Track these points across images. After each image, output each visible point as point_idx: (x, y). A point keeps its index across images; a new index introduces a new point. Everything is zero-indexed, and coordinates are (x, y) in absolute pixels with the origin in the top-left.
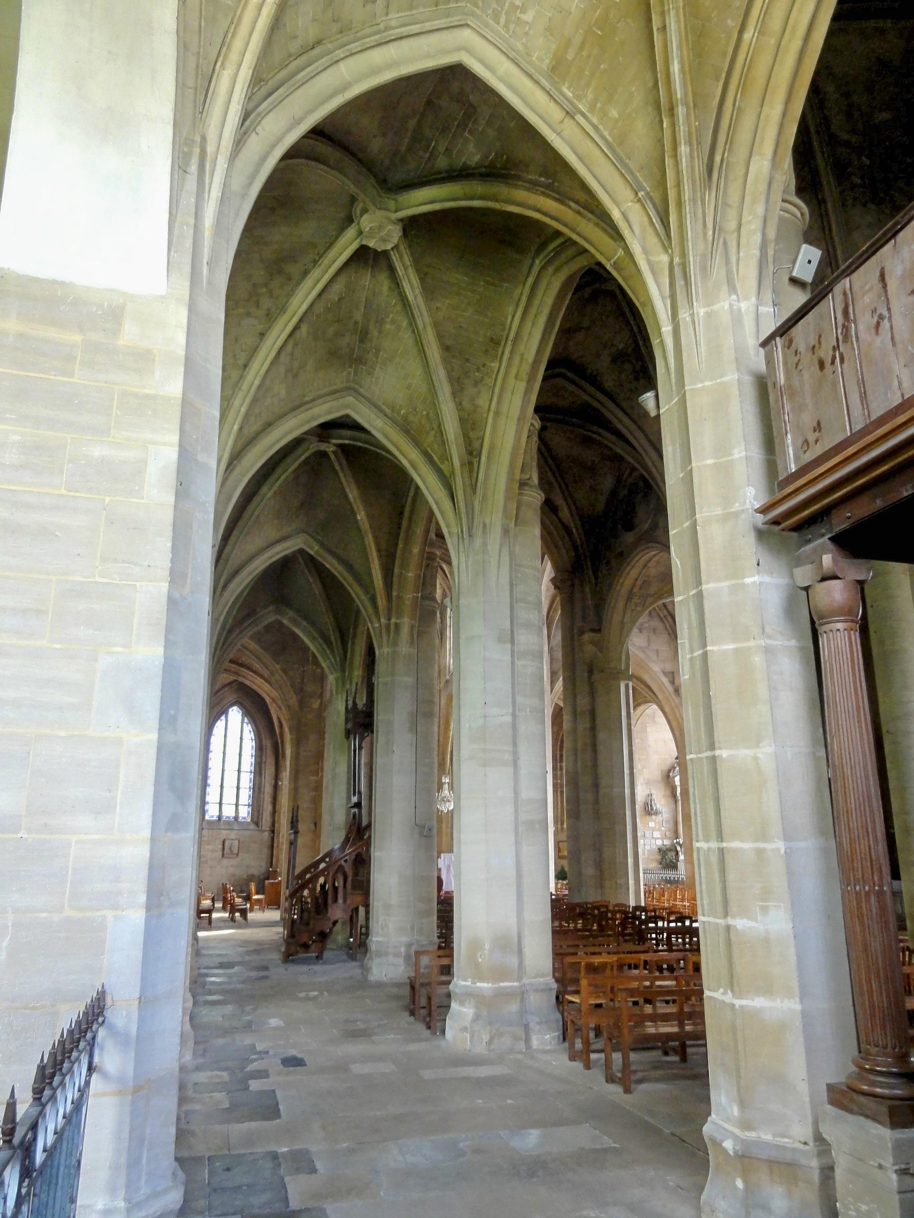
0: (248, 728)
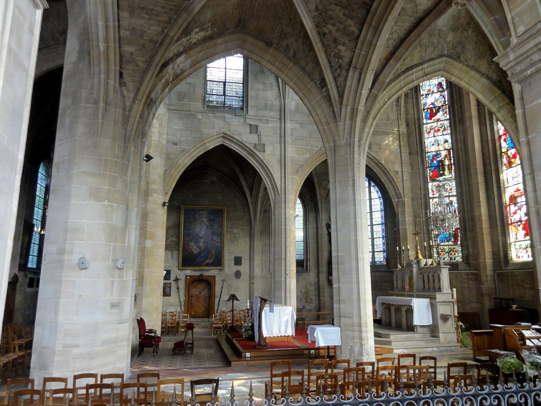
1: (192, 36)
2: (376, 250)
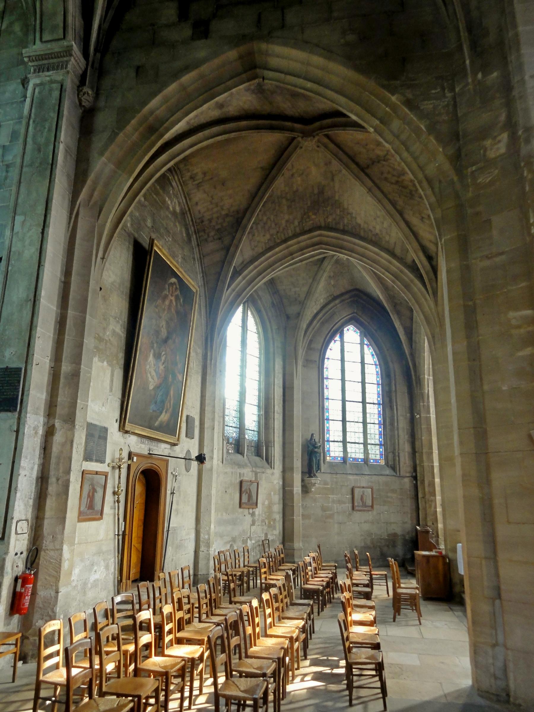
0: (368, 352)
2: (369, 441)
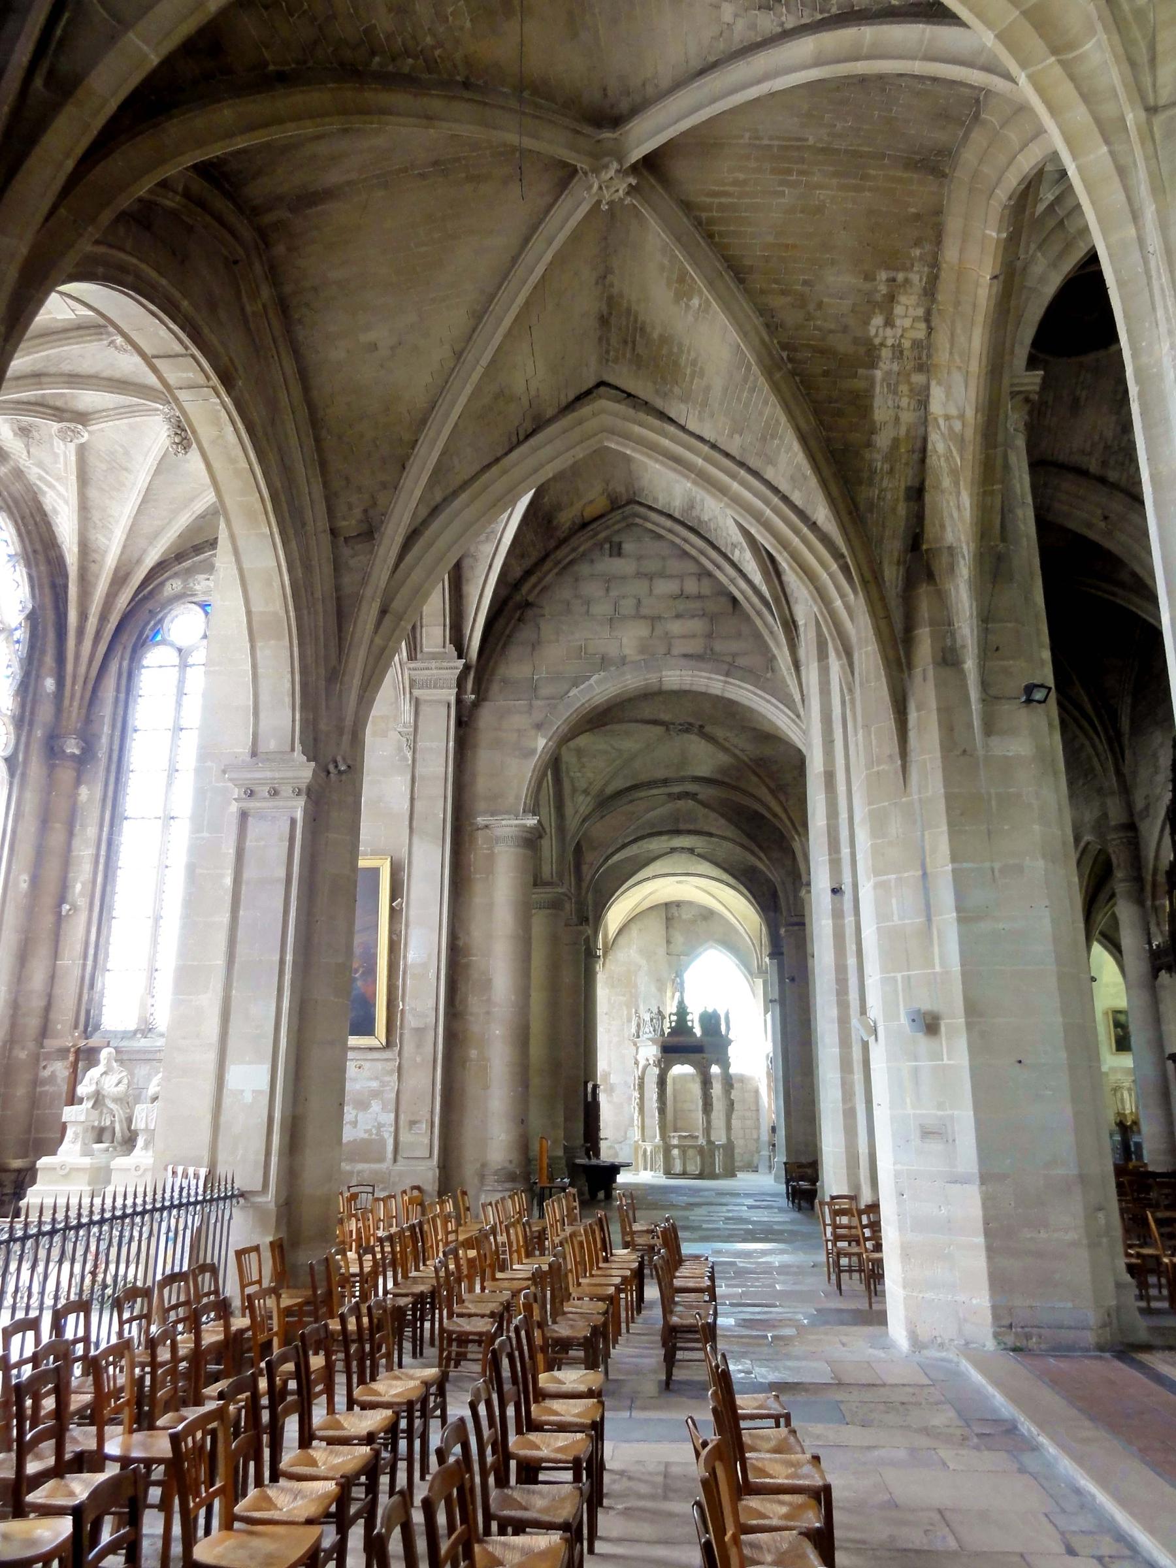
1: (890, 342)
